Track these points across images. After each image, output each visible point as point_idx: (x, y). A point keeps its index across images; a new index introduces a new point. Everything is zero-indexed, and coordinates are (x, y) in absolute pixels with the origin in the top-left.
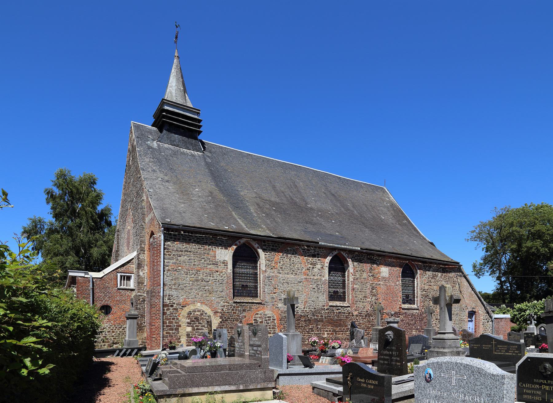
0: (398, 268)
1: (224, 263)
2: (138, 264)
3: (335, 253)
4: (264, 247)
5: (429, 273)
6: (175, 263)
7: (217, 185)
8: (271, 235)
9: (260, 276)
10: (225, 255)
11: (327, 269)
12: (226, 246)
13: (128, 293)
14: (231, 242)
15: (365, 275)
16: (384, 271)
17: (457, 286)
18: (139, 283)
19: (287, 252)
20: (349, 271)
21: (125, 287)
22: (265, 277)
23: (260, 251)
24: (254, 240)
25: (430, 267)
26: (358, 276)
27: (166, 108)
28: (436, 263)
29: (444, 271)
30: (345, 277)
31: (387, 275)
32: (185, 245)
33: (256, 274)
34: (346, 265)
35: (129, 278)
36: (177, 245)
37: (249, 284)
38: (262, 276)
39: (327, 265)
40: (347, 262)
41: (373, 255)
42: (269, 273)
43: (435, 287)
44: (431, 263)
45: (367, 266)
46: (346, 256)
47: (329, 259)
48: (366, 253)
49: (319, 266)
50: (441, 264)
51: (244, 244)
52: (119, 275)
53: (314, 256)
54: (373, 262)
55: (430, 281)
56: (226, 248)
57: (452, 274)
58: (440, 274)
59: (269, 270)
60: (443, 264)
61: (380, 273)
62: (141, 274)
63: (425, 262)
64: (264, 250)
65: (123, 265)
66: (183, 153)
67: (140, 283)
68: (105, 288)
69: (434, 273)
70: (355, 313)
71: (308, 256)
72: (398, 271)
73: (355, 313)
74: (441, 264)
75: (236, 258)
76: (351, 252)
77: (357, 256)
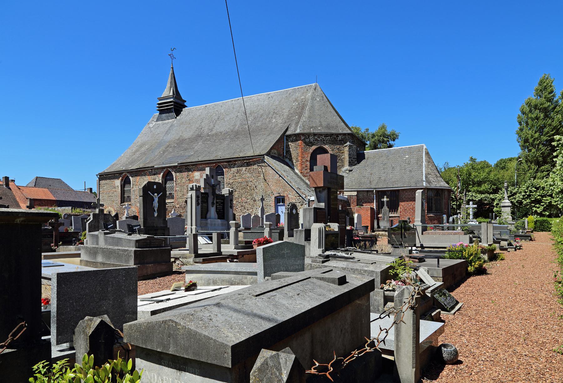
3: (165, 170)
5: (234, 170)
12: (118, 178)
15: (184, 180)
17: (262, 176)
19: (142, 175)
24: (128, 172)
25: (235, 164)
28: (240, 160)
29: (248, 164)
41: (188, 165)
43: (239, 180)
44: (235, 161)
45: (185, 174)
50: (245, 160)
53: (154, 174)
54: (188, 170)
55: (235, 176)
57: (255, 167)
58: (244, 168)
60: (247, 160)
63: (230, 161)
64: (132, 177)
69: (239, 168)
70: (177, 206)
73: (177, 206)
74: (245, 160)
77: (179, 168)
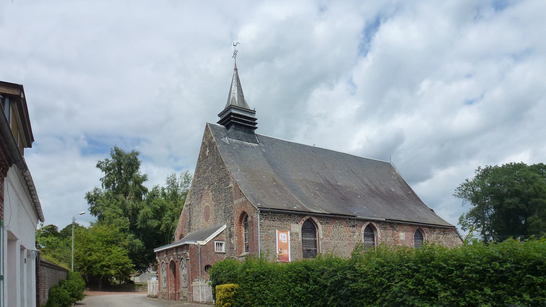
0: (410, 233)
1: (296, 234)
2: (230, 234)
4: (321, 221)
6: (266, 235)
7: (275, 172)
8: (324, 212)
9: (319, 242)
10: (297, 228)
11: (363, 235)
13: (222, 256)
14: (299, 219)
16: (402, 235)
18: (231, 248)
20: (377, 237)
21: (219, 251)
22: (322, 243)
23: (319, 224)
26: (384, 240)
27: (233, 111)
30: (374, 241)
31: (404, 239)
32: (272, 222)
33: (316, 241)
34: (375, 232)
35: (221, 244)
36: (267, 222)
37: (311, 248)
38: (320, 242)
39: (363, 232)
40: (376, 230)
42: (326, 240)
45: (390, 232)
46: (375, 225)
47: (364, 228)
48: (389, 222)
49: (357, 234)
51: (308, 220)
52: (215, 242)
53: (353, 226)
56: (297, 223)
58: (441, 236)
59: (324, 238)
61: (399, 237)
62: (232, 242)
65: (218, 236)
66: (246, 146)
67: (231, 248)
68: (207, 252)
71: (350, 227)
72: (411, 235)
75: (304, 229)
76: (378, 222)
